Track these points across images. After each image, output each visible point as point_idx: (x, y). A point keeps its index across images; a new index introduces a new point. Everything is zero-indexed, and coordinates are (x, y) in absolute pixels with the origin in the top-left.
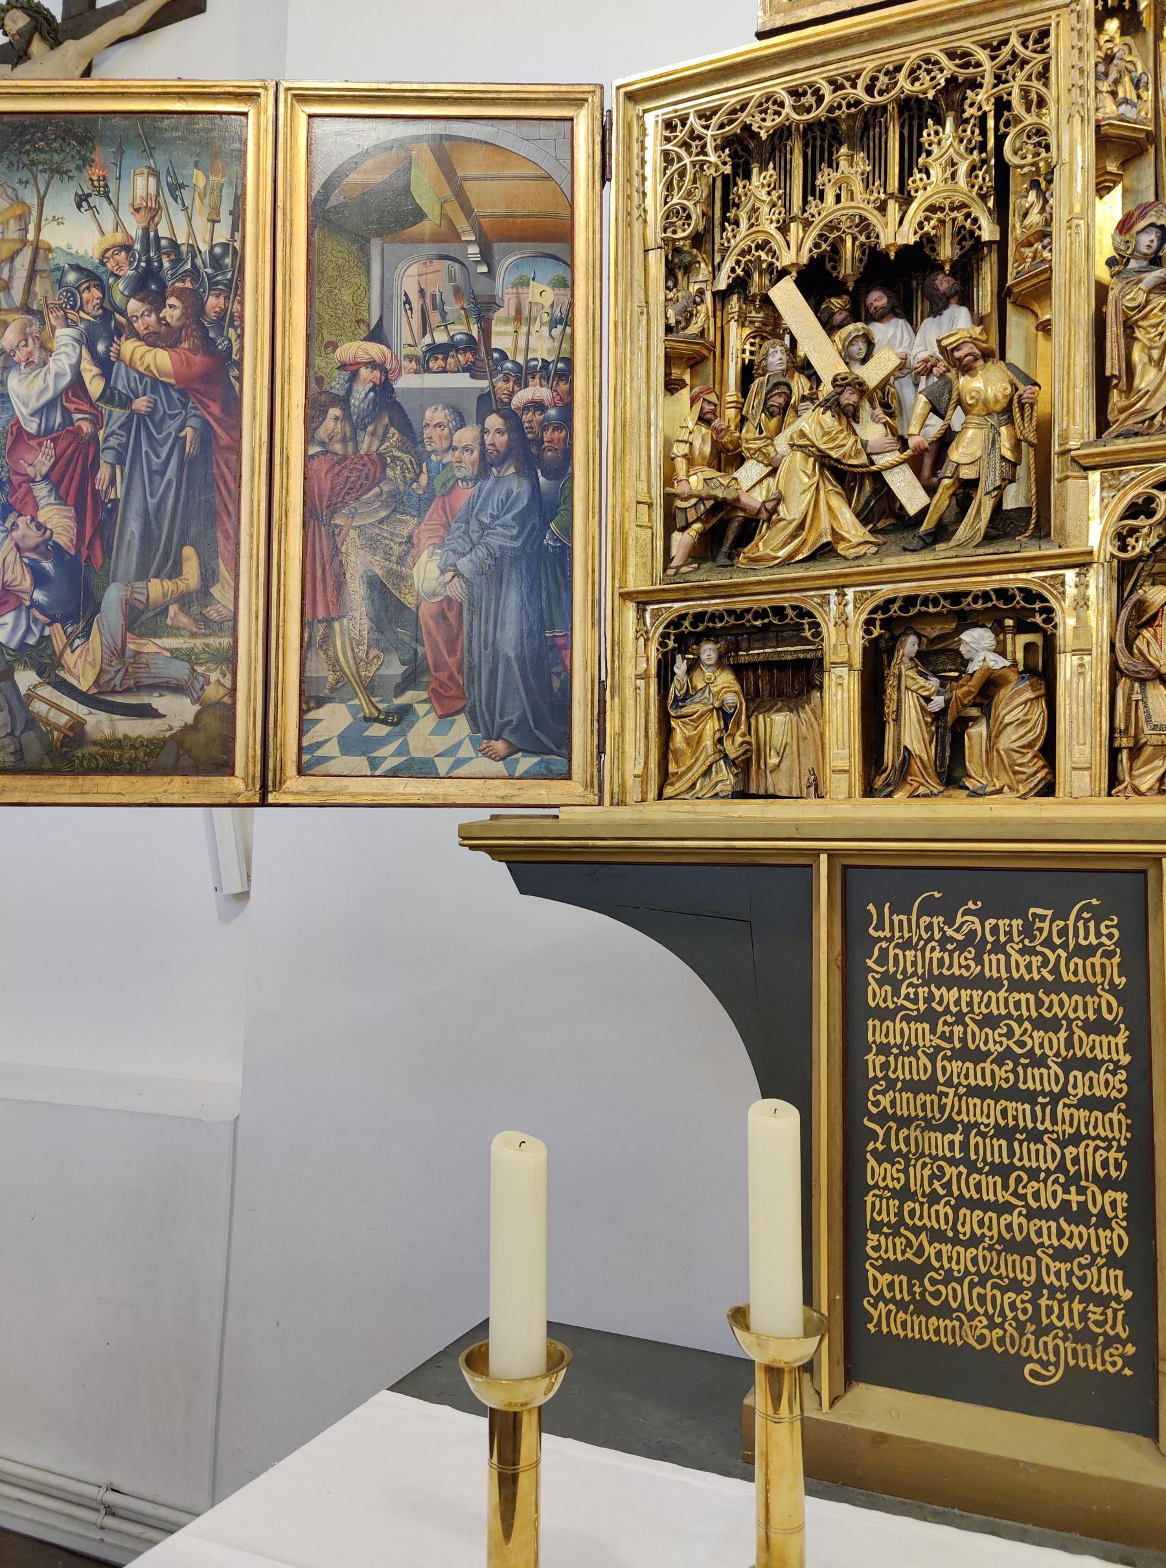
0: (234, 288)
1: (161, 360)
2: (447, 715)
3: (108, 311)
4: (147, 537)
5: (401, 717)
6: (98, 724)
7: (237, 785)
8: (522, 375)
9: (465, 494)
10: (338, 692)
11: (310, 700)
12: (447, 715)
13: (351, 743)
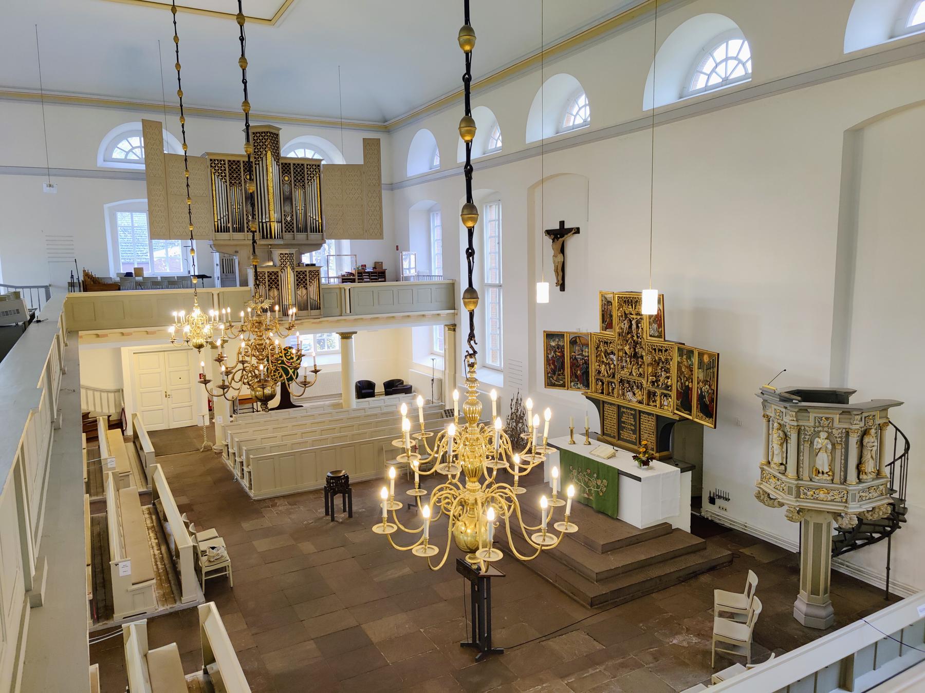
0: (564, 348)
1: (559, 354)
2: (581, 384)
3: (555, 350)
4: (559, 368)
5: (577, 384)
6: (556, 383)
7: (566, 388)
8: (585, 357)
9: (581, 366)
10: (573, 381)
11: (571, 382)
12: (581, 384)
13: (574, 385)
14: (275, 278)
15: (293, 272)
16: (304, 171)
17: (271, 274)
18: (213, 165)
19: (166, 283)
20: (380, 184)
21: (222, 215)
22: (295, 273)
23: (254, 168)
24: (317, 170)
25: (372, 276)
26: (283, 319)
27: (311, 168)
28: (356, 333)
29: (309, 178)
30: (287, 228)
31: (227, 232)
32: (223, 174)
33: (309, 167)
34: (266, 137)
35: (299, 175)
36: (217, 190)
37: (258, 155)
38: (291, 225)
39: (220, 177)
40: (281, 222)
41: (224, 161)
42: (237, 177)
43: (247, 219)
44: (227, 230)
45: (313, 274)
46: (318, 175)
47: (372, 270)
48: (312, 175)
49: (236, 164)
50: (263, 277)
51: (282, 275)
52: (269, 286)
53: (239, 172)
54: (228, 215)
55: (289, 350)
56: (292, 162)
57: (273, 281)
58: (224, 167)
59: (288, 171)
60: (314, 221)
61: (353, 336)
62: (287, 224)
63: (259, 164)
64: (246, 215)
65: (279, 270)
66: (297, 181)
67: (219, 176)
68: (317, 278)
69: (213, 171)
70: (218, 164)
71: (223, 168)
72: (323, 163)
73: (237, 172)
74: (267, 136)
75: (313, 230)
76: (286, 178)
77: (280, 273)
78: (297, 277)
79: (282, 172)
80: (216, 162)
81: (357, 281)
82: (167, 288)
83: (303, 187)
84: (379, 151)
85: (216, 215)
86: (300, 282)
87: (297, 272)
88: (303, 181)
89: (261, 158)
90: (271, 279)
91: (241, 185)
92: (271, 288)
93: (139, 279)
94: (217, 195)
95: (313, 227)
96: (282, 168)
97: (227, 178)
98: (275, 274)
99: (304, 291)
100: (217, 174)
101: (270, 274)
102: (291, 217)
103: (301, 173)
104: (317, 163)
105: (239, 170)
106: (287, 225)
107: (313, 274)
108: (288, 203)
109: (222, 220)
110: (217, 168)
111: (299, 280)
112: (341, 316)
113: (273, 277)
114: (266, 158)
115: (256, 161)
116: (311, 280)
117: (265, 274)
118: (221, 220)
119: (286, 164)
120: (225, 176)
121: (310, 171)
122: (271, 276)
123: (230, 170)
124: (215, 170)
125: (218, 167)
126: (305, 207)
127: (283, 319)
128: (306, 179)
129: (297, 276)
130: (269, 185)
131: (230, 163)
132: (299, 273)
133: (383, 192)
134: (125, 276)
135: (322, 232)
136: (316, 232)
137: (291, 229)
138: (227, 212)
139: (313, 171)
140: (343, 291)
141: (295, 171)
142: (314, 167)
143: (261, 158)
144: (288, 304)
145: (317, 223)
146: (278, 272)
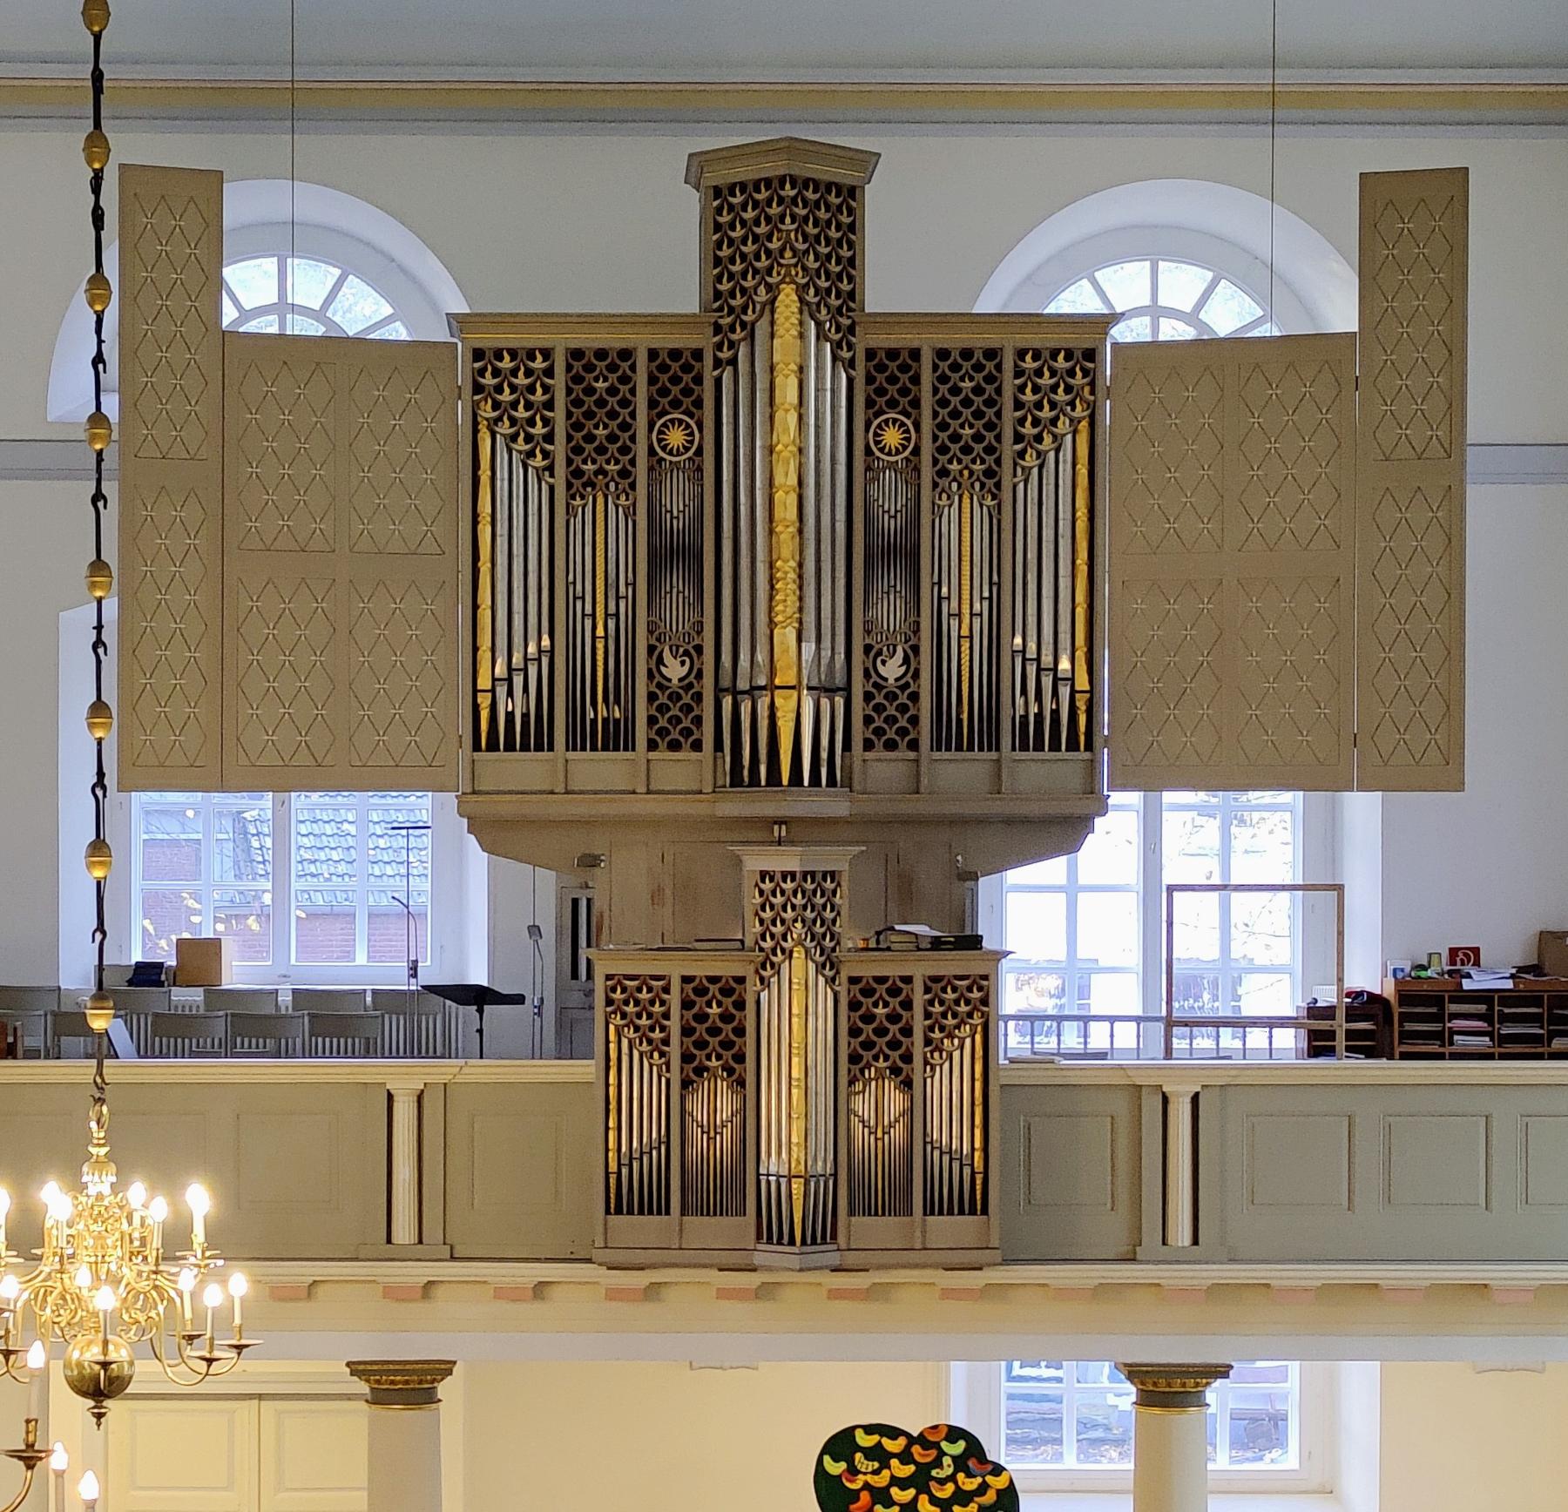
14: (726, 1018)
15: (831, 981)
16: (999, 391)
17: (701, 991)
18: (489, 380)
19: (219, 1029)
20: (1453, 446)
21: (517, 659)
22: (843, 990)
23: (708, 384)
24: (1079, 380)
25: (1505, 1019)
26: (758, 1259)
27: (1039, 373)
28: (1222, 1371)
29: (1028, 430)
30: (879, 722)
31: (539, 748)
32: (539, 430)
33: (1029, 363)
34: (775, 210)
35: (967, 413)
36: (502, 515)
37: (731, 310)
38: (903, 709)
39: (521, 445)
40: (847, 689)
41: (547, 354)
42: (612, 438)
44: (535, 737)
46: (1079, 411)
47: (1509, 984)
48: (1046, 413)
49: (613, 368)
50: (657, 1009)
51: (764, 995)
52: (687, 1058)
53: (625, 412)
54: (552, 651)
55: (944, 1445)
56: (927, 342)
57: (713, 1031)
58: (546, 389)
59: (904, 392)
60: (1047, 681)
61: (1210, 1396)
63: (733, 362)
64: (651, 649)
65: (748, 971)
66: (955, 448)
67: (514, 438)
68: (977, 1020)
69: (487, 412)
70: (514, 373)
71: (539, 397)
72: (1122, 333)
73: (613, 415)
74: (781, 201)
75: (1030, 737)
76: (892, 437)
77: (752, 985)
79: (870, 403)
80: (506, 364)
81: (1341, 1042)
82: (228, 1049)
83: (990, 483)
84: (1458, 248)
86: (868, 1045)
87: (853, 980)
88: (990, 450)
89: (744, 325)
90: (702, 1017)
91: (633, 486)
92: (699, 1071)
93: (188, 997)
94: (502, 543)
95: (1055, 714)
96: (870, 380)
97: (559, 449)
99: (895, 1101)
100: (505, 428)
101: (696, 988)
102: (906, 661)
103: (978, 400)
104: (1080, 342)
105: (625, 403)
106: (879, 708)
107: (950, 996)
108: (895, 578)
109: (518, 680)
110: (506, 396)
111: (868, 1029)
112: (1133, 1260)
113: (715, 1010)
114: (772, 323)
115: (719, 347)
116: (937, 1035)
117: (666, 990)
118: (510, 680)
119: (893, 354)
120: (549, 438)
121: (1036, 389)
123: (578, 403)
124: (496, 407)
125: (513, 388)
126: (994, 603)
127: (758, 1259)
128: (1008, 435)
129: (854, 1005)
130: (779, 479)
131: (578, 366)
132: (868, 992)
133: (1476, 497)
134: (130, 983)
135: (1089, 747)
136: (1055, 747)
137: (903, 732)
138: (546, 642)
139: (1054, 388)
140: (1152, 1105)
141: (944, 389)
142: (1061, 363)
143: (744, 325)
144: (773, 1170)
145: (1064, 692)
146: (741, 980)
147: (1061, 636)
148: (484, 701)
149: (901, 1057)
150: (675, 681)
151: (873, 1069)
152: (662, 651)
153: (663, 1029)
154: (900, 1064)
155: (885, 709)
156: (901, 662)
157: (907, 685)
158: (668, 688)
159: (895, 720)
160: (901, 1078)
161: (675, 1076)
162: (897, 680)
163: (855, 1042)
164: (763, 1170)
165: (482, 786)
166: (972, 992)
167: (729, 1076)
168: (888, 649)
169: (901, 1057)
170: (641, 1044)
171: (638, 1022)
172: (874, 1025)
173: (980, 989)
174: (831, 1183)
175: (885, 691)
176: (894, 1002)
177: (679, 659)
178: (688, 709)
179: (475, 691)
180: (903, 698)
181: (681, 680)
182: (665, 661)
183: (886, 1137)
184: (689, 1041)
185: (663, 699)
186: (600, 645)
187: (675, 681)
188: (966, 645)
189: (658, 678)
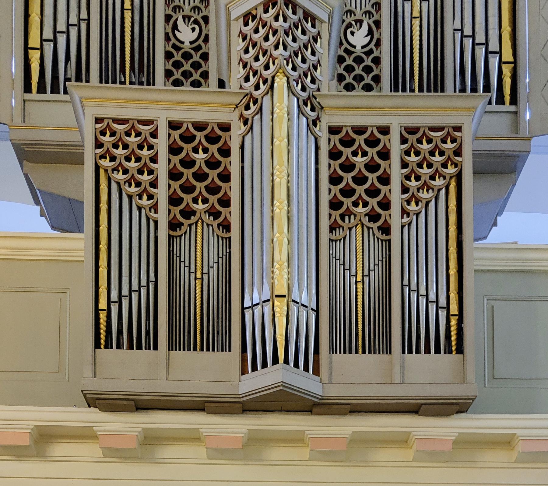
14: (212, 164)
17: (188, 138)
21: (62, 27)
22: (322, 131)
43: (167, 38)
45: (425, 146)
52: (174, 201)
57: (200, 176)
60: (481, 52)
62: (349, 61)
64: (168, 18)
78: (336, 164)
85: (35, 18)
86: (348, 192)
87: (334, 130)
90: (188, 163)
98: (212, 139)
102: (370, 32)
107: (425, 146)
111: (348, 177)
113: (201, 156)
117: (154, 135)
118: (55, 41)
122: (187, 148)
129: (334, 155)
146: (226, 128)
147: (490, 20)
148: (35, 56)
149: (379, 204)
150: (187, 44)
151: (352, 217)
152: (177, 19)
153: (151, 172)
154: (379, 210)
155: (354, 69)
156: (366, 33)
157: (371, 52)
158: (181, 48)
159: (361, 78)
160: (379, 223)
161: (162, 217)
162: (363, 47)
163: (336, 189)
164: (247, 304)
165: (26, 102)
166: (446, 143)
167: (214, 220)
168: (356, 24)
169: (379, 204)
170: (130, 185)
171: (127, 164)
172: (353, 174)
173: (453, 141)
174: (313, 316)
175: (353, 56)
176: (372, 152)
177: (190, 27)
178: (196, 66)
179: (26, 48)
180: (368, 62)
181: (191, 43)
182: (179, 28)
183: (366, 279)
184: (176, 185)
185: (178, 57)
186: (128, 15)
187: (187, 44)
188: (416, 22)
189: (173, 40)
